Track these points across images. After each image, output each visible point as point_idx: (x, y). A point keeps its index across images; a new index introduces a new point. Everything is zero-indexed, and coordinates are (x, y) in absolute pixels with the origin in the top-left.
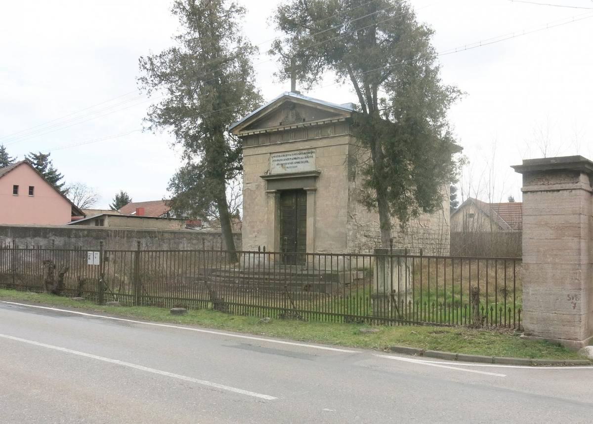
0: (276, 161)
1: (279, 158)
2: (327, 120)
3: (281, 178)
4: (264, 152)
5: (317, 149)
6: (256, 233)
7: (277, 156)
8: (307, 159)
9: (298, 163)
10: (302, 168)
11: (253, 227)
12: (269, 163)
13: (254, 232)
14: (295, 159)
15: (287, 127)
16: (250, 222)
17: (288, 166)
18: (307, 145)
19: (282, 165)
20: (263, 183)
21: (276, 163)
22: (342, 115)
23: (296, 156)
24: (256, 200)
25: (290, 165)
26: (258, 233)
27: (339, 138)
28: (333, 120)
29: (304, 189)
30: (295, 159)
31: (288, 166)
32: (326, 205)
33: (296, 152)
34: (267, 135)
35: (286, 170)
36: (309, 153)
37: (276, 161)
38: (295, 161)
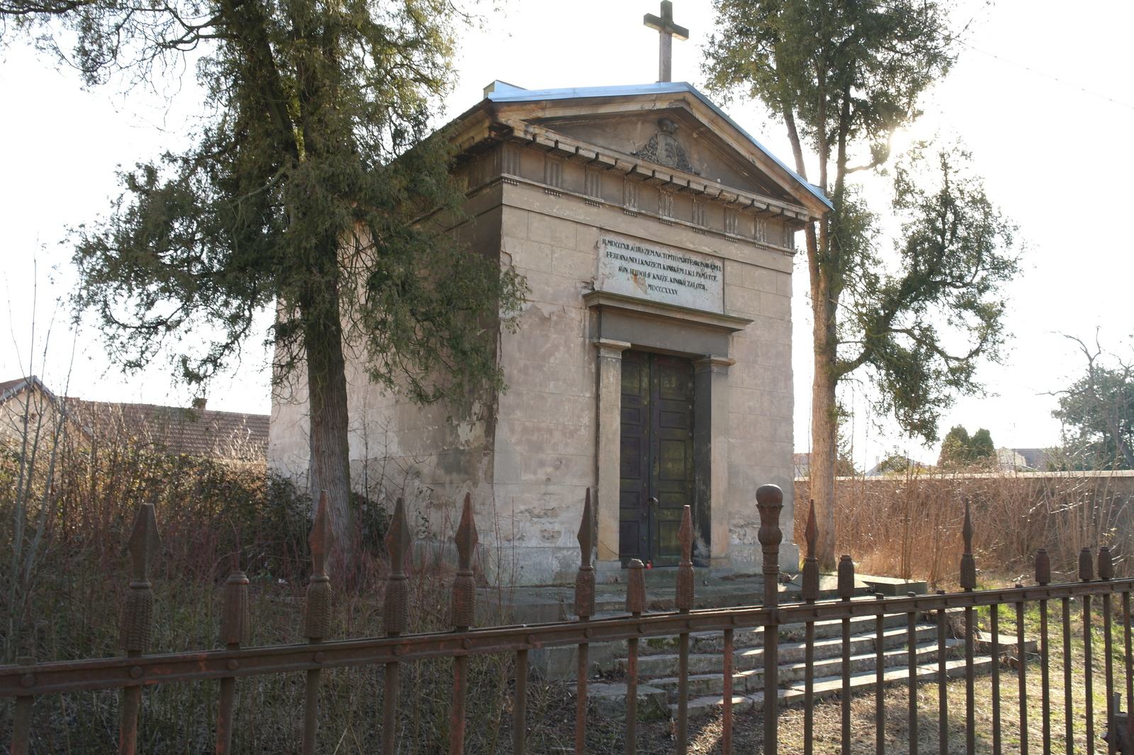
0: (616, 256)
1: (628, 254)
2: (762, 202)
3: (658, 312)
4: (581, 218)
5: (727, 263)
6: (549, 470)
7: (619, 246)
8: (702, 281)
9: (680, 282)
10: (686, 298)
11: (537, 447)
12: (598, 259)
13: (542, 464)
14: (671, 269)
15: (679, 178)
16: (525, 430)
17: (650, 281)
18: (707, 244)
19: (635, 274)
20: (578, 317)
21: (618, 263)
22: (801, 204)
23: (674, 264)
24: (552, 360)
25: (656, 283)
26: (557, 468)
27: (775, 255)
28: (788, 210)
29: (712, 358)
30: (671, 269)
31: (650, 281)
32: (749, 407)
33: (673, 252)
34: (592, 165)
35: (646, 292)
36: (707, 266)
37: (616, 256)
38: (671, 274)
